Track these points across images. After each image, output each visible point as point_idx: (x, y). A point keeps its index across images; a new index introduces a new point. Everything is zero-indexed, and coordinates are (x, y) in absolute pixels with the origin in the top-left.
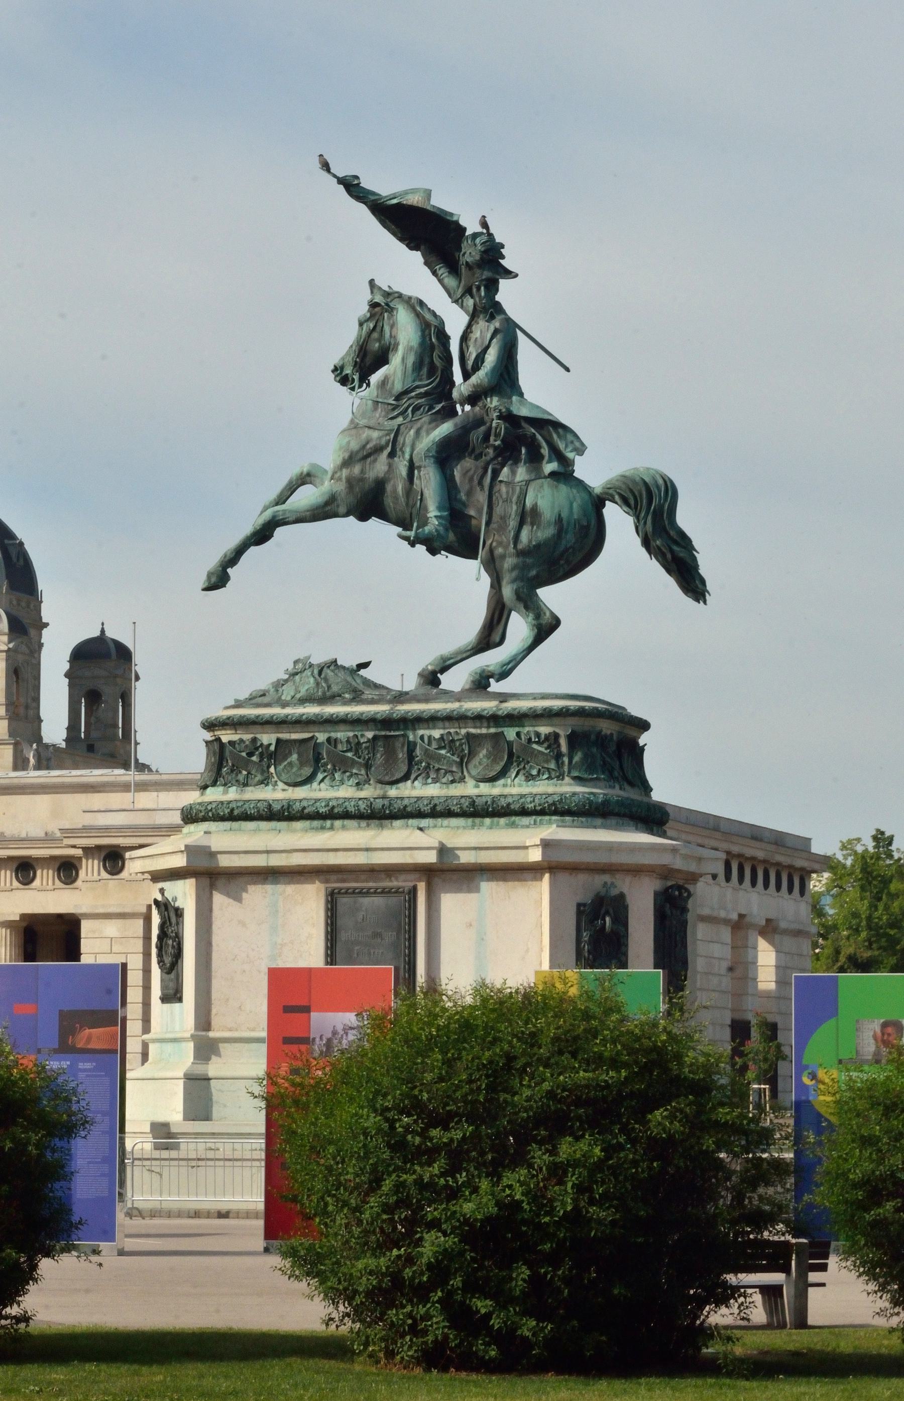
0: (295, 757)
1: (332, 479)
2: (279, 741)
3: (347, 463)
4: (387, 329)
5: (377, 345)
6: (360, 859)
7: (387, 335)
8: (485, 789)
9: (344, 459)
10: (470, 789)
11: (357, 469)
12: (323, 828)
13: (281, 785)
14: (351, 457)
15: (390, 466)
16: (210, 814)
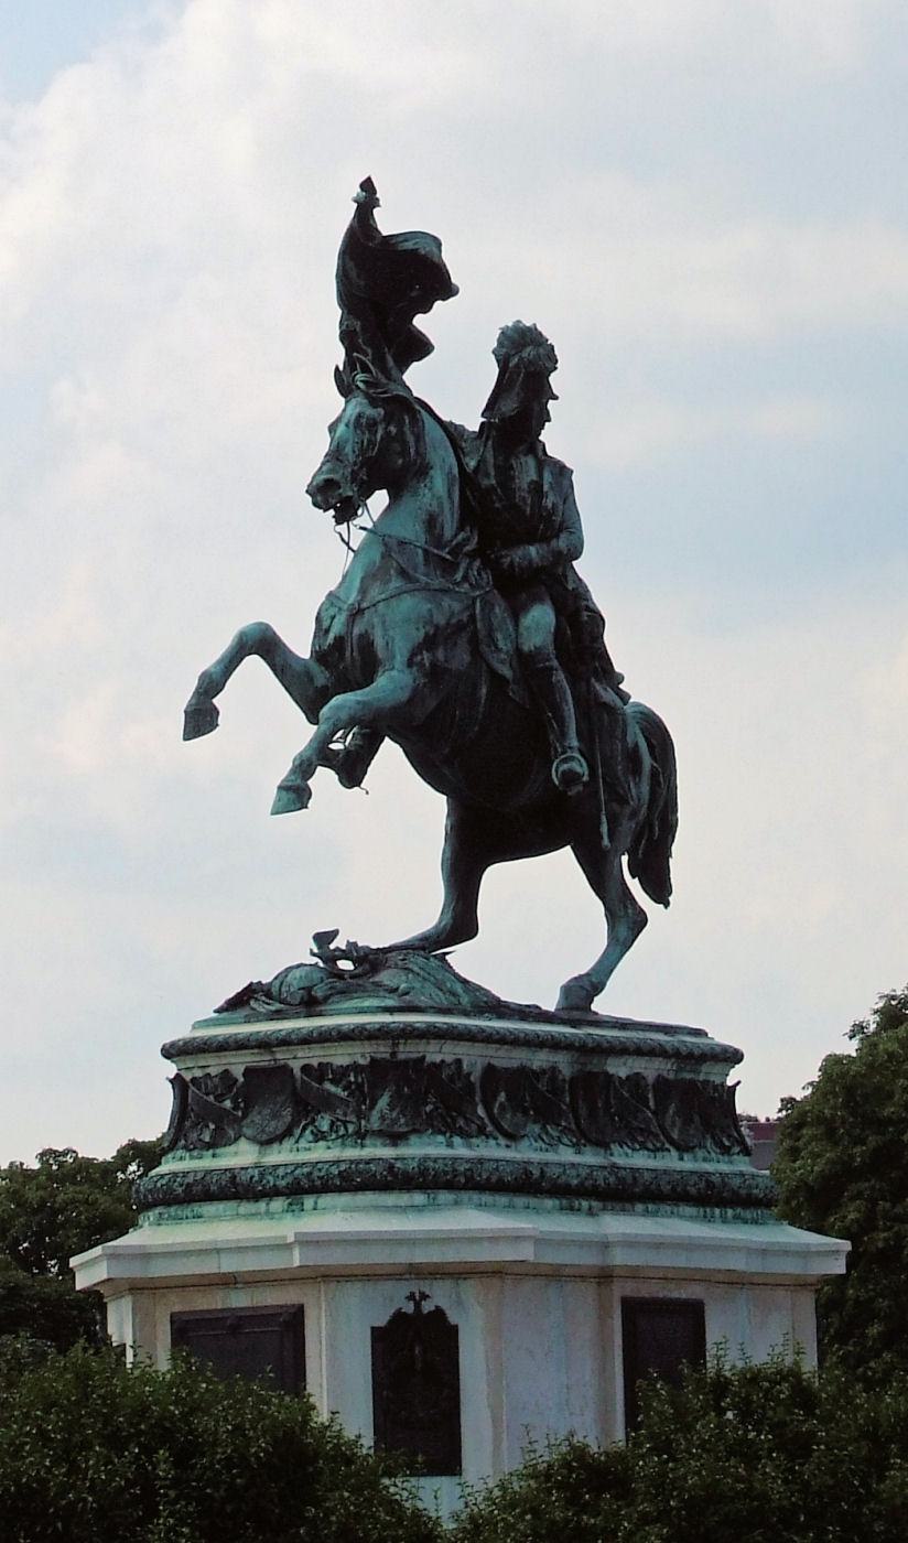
0: (502, 1097)
1: (410, 663)
2: (490, 1070)
3: (429, 643)
4: (411, 439)
5: (400, 461)
6: (680, 1261)
7: (412, 451)
8: (688, 1164)
9: (427, 634)
10: (671, 1161)
11: (440, 654)
12: (572, 1209)
13: (502, 1141)
14: (435, 635)
15: (476, 653)
16: (463, 1180)
